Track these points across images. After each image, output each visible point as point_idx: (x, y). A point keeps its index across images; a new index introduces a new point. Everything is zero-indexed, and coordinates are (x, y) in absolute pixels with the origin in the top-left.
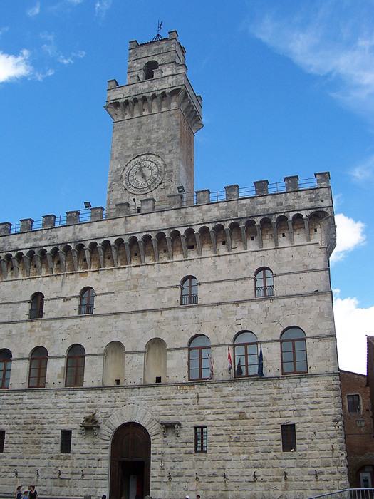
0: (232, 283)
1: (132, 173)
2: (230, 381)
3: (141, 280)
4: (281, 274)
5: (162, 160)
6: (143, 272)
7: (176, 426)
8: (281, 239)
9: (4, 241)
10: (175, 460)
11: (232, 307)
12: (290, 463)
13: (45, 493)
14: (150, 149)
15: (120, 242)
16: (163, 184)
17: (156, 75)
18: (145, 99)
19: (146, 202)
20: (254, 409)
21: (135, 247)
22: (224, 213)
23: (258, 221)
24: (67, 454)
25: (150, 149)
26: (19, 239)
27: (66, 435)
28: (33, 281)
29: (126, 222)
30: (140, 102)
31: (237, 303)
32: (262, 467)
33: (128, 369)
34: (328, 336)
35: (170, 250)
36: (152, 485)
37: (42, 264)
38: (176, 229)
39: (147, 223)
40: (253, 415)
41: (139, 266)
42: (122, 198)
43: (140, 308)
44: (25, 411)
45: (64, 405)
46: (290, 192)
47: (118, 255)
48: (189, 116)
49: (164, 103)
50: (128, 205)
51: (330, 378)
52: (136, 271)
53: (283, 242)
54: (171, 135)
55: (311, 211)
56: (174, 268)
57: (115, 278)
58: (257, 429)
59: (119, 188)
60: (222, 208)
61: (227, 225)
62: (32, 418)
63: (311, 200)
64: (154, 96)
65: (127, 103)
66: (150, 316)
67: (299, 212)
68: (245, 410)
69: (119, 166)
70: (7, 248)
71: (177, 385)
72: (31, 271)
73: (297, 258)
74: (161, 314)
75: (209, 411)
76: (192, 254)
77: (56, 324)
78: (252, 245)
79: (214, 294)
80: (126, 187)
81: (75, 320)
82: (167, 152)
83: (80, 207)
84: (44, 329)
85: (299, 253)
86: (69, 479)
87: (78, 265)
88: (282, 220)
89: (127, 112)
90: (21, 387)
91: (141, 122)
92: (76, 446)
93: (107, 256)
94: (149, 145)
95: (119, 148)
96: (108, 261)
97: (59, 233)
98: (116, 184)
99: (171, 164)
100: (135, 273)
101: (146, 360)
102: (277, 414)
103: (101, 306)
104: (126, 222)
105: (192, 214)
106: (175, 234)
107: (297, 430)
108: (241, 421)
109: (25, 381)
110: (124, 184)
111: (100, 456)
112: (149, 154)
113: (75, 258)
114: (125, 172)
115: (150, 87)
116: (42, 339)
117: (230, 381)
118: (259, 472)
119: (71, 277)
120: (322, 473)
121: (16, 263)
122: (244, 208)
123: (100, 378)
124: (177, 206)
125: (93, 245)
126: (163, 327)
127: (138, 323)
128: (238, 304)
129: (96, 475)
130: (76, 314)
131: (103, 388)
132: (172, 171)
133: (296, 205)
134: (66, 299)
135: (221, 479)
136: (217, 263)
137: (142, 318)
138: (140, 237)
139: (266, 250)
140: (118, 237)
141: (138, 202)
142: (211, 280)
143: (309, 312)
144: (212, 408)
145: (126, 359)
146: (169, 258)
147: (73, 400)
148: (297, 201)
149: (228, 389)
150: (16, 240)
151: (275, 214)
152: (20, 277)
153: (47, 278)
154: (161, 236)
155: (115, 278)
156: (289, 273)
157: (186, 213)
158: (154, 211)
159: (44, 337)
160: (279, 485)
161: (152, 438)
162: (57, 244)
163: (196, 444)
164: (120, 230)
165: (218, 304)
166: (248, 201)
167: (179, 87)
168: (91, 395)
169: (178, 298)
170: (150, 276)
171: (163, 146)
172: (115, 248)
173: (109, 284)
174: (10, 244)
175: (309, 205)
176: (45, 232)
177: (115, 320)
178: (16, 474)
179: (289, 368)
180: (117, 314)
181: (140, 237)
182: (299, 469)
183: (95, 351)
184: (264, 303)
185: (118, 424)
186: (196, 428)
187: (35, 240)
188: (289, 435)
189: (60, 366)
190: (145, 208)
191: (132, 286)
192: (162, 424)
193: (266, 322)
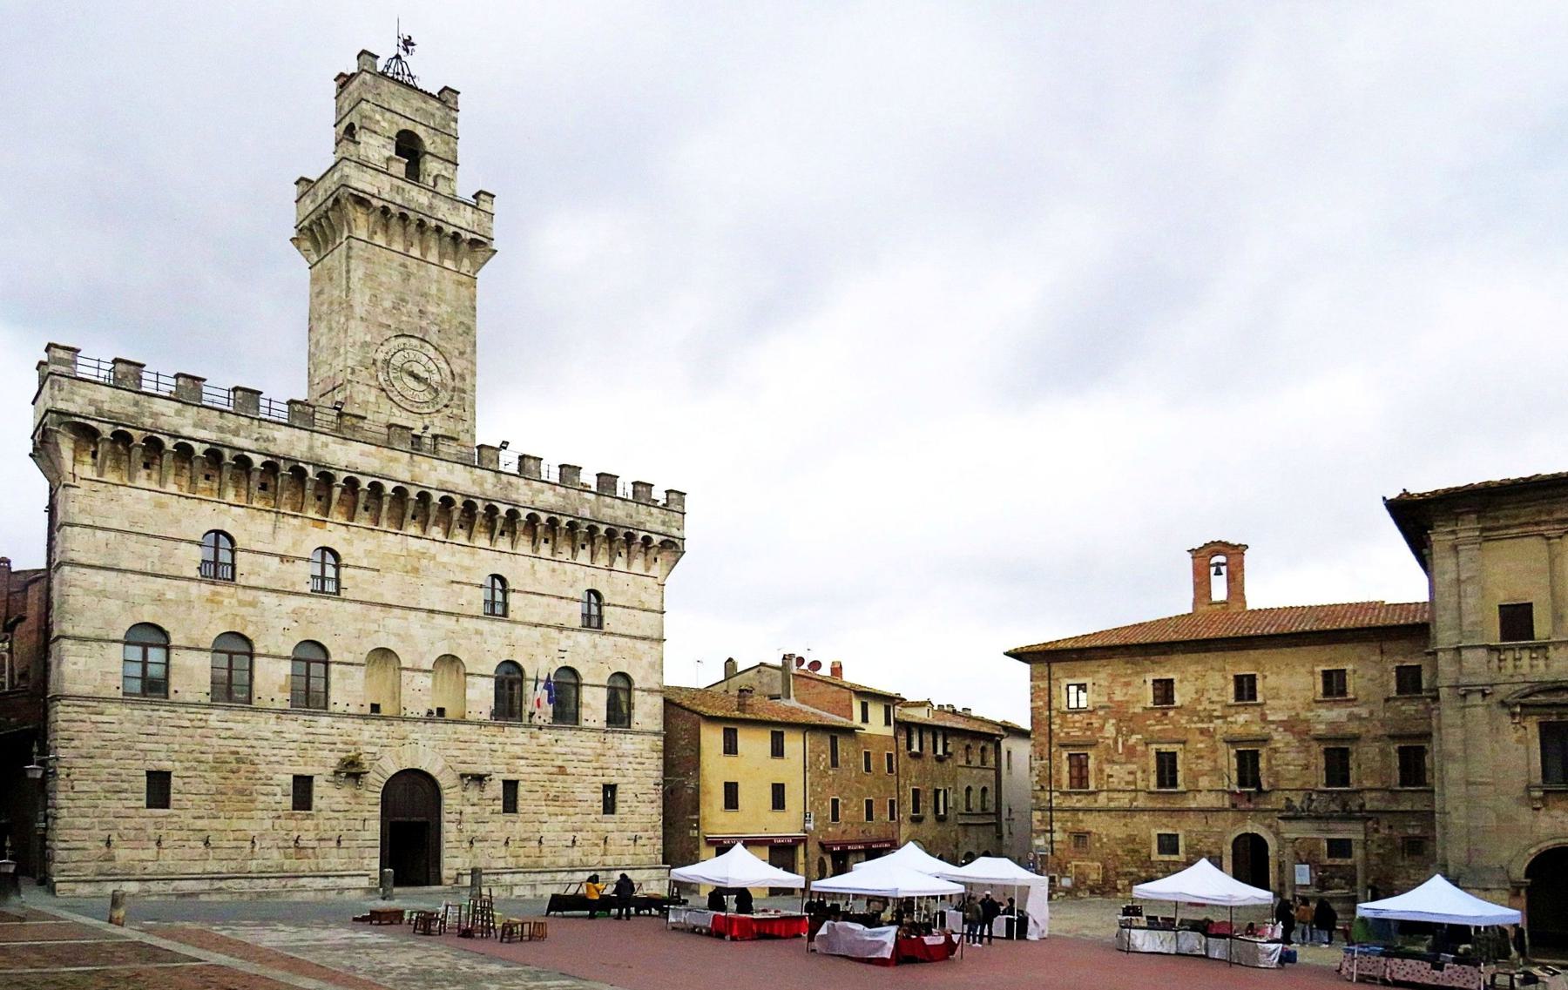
20: (575, 763)
30: (412, 228)
45: (295, 736)
58: (578, 788)
71: (480, 724)
75: (523, 762)
91: (405, 266)
101: (435, 679)
102: (600, 772)
131: (363, 717)
168: (347, 725)
192: (463, 776)
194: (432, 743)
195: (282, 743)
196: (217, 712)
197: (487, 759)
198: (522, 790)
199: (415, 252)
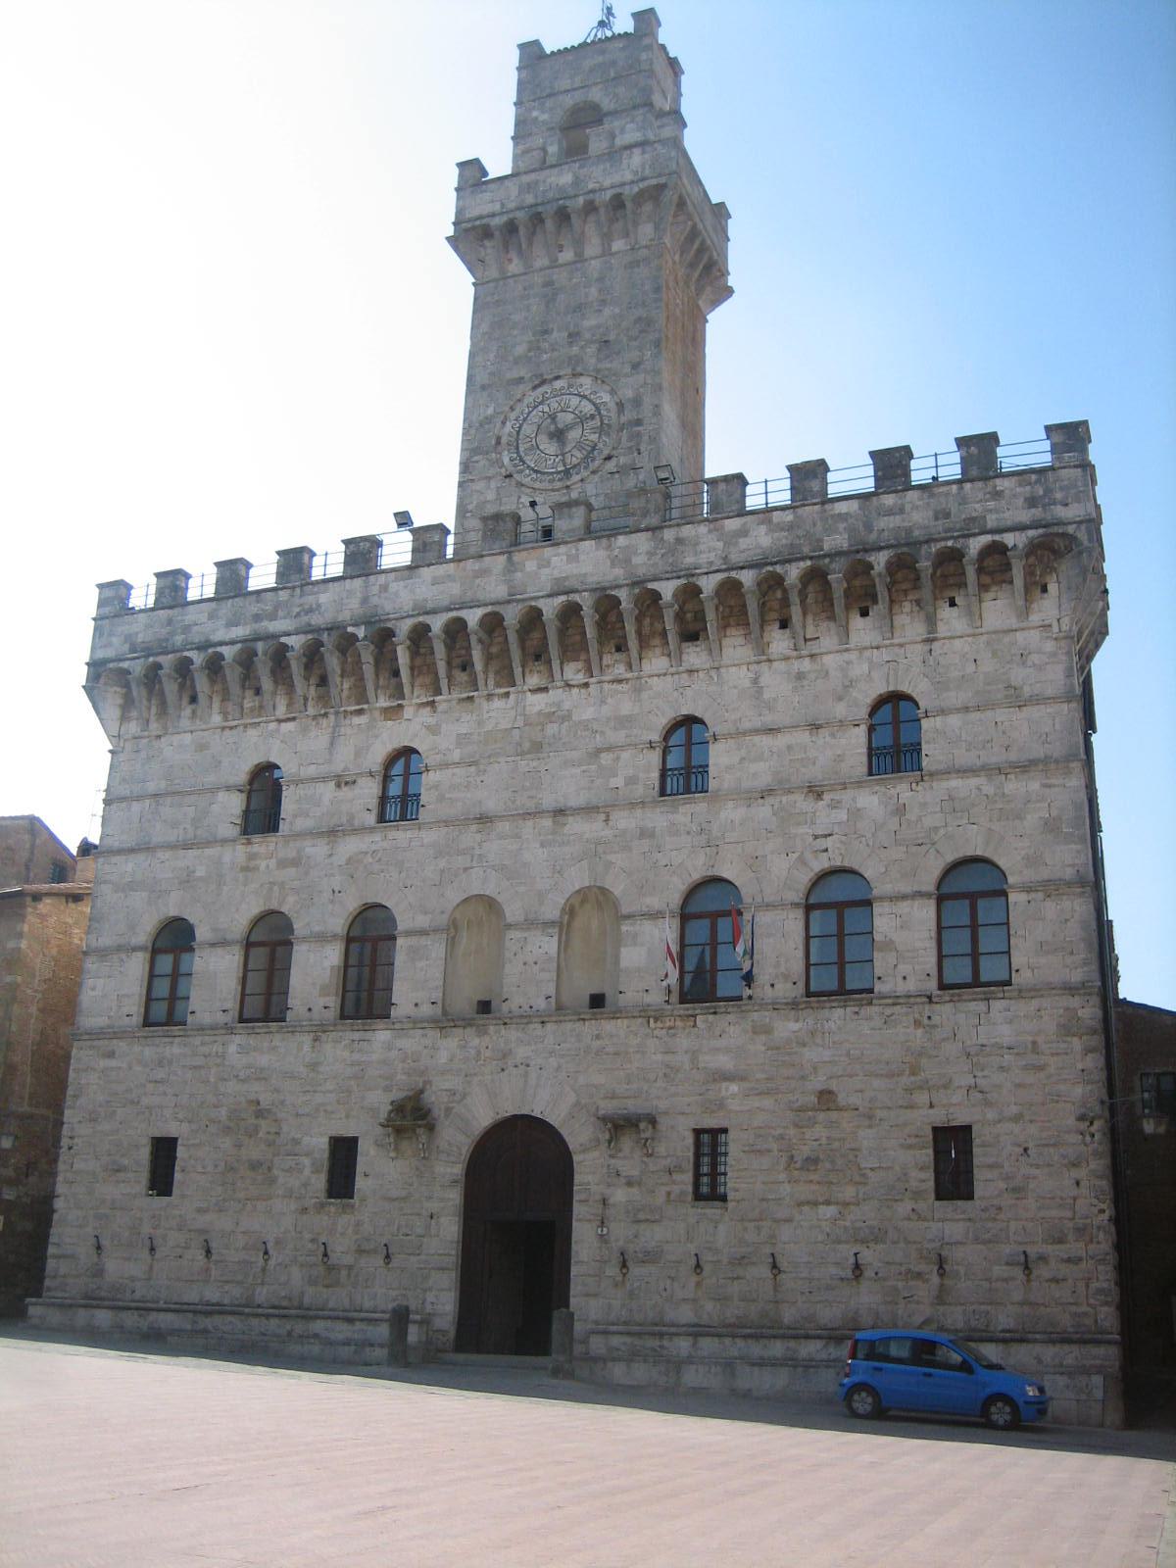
0: (803, 737)
1: (528, 429)
2: (794, 1005)
3: (552, 729)
4: (942, 712)
5: (613, 392)
6: (558, 704)
7: (642, 1125)
8: (945, 613)
9: (170, 622)
10: (641, 1216)
11: (802, 802)
12: (955, 1230)
13: (285, 1303)
14: (575, 361)
15: (493, 623)
16: (614, 462)
17: (597, 145)
18: (563, 216)
19: (566, 510)
21: (536, 635)
22: (784, 538)
23: (880, 560)
24: (345, 1201)
25: (575, 361)
26: (212, 616)
27: (343, 1151)
28: (252, 732)
29: (511, 567)
30: (549, 224)
31: (815, 791)
32: (877, 1237)
33: (512, 971)
34: (1069, 884)
35: (633, 643)
36: (575, 1288)
37: (276, 682)
38: (650, 586)
39: (572, 569)
40: (855, 1100)
41: (545, 689)
42: (499, 499)
43: (548, 801)
44: (232, 1087)
46: (971, 481)
47: (488, 659)
48: (692, 265)
49: (618, 226)
50: (517, 520)
51: (1075, 1002)
52: (537, 703)
53: (951, 620)
54: (639, 319)
55: (1031, 533)
56: (645, 695)
57: (480, 723)
58: (867, 1138)
59: (491, 472)
60: (780, 527)
61: (793, 573)
62: (250, 1102)
63: (1032, 502)
64: (590, 208)
65: (511, 228)
66: (575, 826)
67: (997, 537)
68: (833, 1085)
69: (490, 411)
70: (179, 639)
71: (648, 1014)
72: (247, 704)
73: (988, 666)
74: (607, 821)
75: (734, 1088)
76: (695, 656)
77: (317, 850)
78: (863, 630)
79: (754, 767)
80: (511, 469)
81: (368, 839)
82: (627, 369)
83: (380, 524)
84: (283, 864)
85: (994, 653)
86: (350, 1268)
87: (377, 688)
88: (952, 558)
89: (513, 254)
90: (221, 1018)
91: (549, 284)
92: (370, 1181)
93: (457, 661)
94: (575, 349)
95: (492, 356)
96: (461, 677)
97: (323, 598)
98: (481, 462)
99: (637, 402)
100: (536, 709)
101: (564, 945)
102: (922, 1098)
103: (441, 798)
104: (511, 567)
105: (697, 544)
106: (650, 601)
107: (976, 1142)
108: (821, 1116)
109: (232, 1004)
110: (506, 460)
111: (433, 1206)
112: (575, 375)
113: (368, 670)
114: (508, 427)
115: (577, 182)
116: (276, 888)
117: (794, 1005)
118: (868, 1256)
119: (356, 720)
120: (1043, 1259)
121: (202, 684)
122: (842, 526)
123: (437, 995)
124: (653, 520)
125: (420, 634)
126: (612, 858)
127: (542, 845)
128: (819, 796)
129: (423, 1257)
130: (371, 819)
132: (639, 422)
133: (988, 517)
134: (342, 781)
135: (765, 1271)
136: (764, 681)
137: (554, 833)
138: (550, 608)
139: (901, 645)
140: (489, 609)
141: (544, 511)
142: (746, 725)
143: (1019, 817)
144: (743, 1079)
145: (508, 944)
146: (630, 666)
147: (356, 1056)
148: (991, 504)
149: (788, 1027)
150: (203, 618)
151: (927, 542)
152: (217, 719)
153: (290, 726)
154: (607, 604)
155: (480, 723)
156: (966, 709)
157: (679, 541)
158: (589, 532)
159: (282, 885)
160: (924, 1291)
161: (576, 1158)
162: (319, 630)
163: (697, 1175)
164: (494, 588)
165: (765, 793)
166: (854, 505)
167: (662, 180)
169: (655, 775)
170: (575, 718)
171: (618, 353)
172: (480, 641)
173: (462, 740)
174: (187, 629)
175: (1025, 516)
176: (283, 595)
177: (478, 837)
178: (208, 1252)
179: (959, 971)
180: (484, 820)
181: (550, 608)
182: (980, 1246)
183: (422, 921)
184: (893, 792)
185: (483, 1117)
186: (698, 1132)
187: (257, 618)
188: (953, 1158)
189: (327, 964)
190: (561, 526)
191: (527, 745)
193: (895, 838)
194: (553, 1062)
195: (329, 1078)
196: (237, 1039)
197: (660, 1083)
198: (735, 1147)
199: (567, 255)
